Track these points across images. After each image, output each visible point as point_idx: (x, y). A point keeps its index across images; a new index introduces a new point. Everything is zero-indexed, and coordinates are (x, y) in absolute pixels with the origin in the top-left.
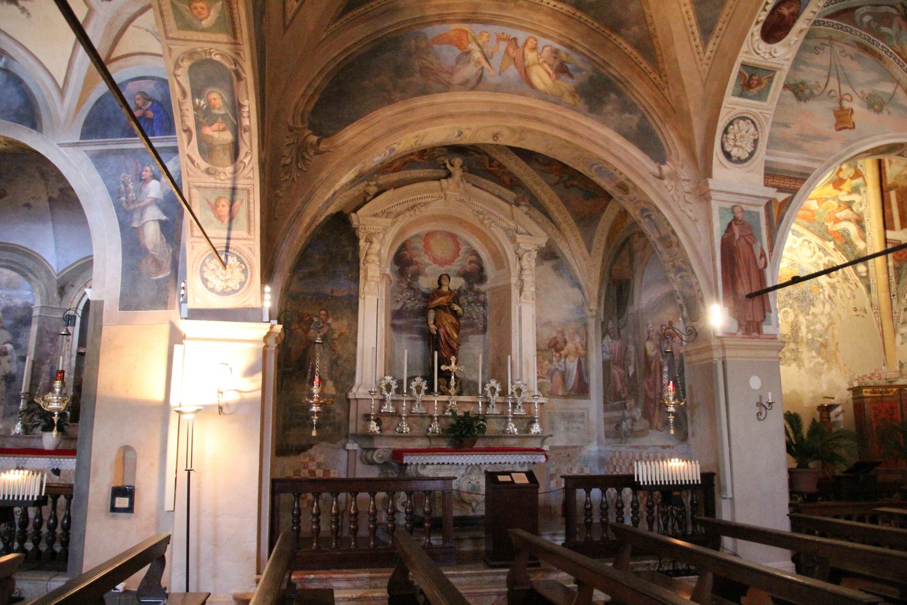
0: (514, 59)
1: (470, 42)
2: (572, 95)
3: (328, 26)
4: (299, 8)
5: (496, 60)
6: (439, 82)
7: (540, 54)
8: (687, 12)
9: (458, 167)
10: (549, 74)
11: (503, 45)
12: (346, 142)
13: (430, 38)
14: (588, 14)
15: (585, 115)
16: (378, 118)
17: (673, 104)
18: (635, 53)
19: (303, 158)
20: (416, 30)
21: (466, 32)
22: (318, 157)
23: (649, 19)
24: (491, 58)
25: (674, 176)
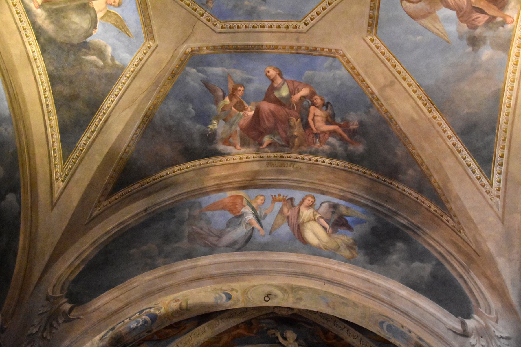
0: (288, 217)
1: (244, 206)
2: (350, 247)
3: (99, 202)
4: (65, 188)
5: (268, 222)
6: (205, 245)
7: (317, 211)
8: (454, 145)
9: (292, 341)
10: (325, 228)
11: (278, 206)
12: (98, 308)
13: (204, 206)
14: (364, 167)
15: (365, 268)
16: (135, 284)
17: (474, 247)
18: (420, 197)
19: (51, 326)
20: (193, 200)
21: (242, 198)
22: (67, 324)
23: (418, 159)
24: (264, 219)
25: (484, 333)
